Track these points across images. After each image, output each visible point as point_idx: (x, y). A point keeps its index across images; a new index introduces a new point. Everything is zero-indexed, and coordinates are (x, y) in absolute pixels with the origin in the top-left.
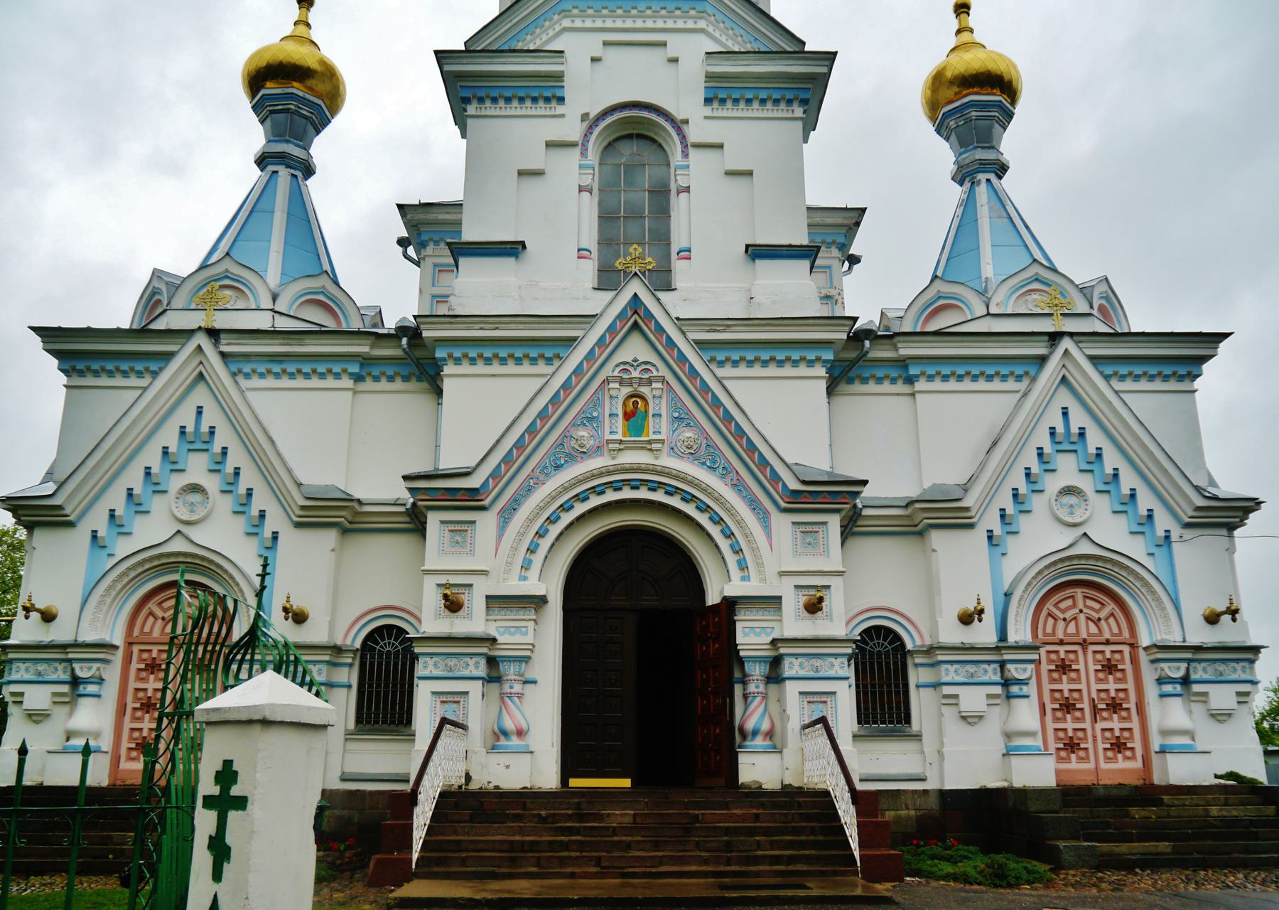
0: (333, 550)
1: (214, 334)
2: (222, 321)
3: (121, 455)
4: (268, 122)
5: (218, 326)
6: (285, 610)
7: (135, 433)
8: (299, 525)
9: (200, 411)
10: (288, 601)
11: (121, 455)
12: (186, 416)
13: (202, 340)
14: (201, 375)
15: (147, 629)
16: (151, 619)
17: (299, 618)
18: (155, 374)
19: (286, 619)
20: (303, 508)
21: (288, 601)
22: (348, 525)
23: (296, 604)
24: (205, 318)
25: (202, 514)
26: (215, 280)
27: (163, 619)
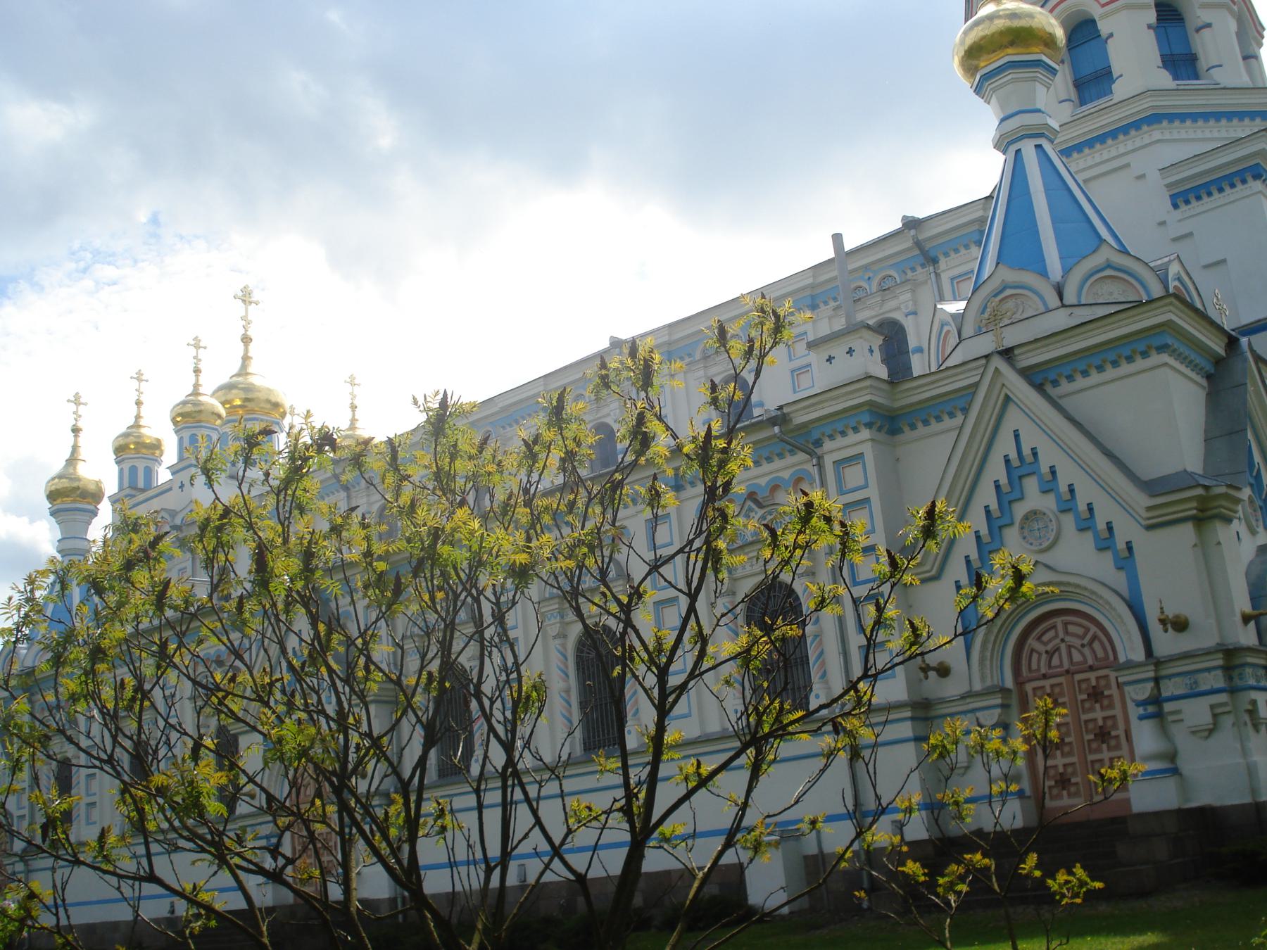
0: (1195, 545)
1: (1007, 353)
2: (1012, 337)
3: (964, 487)
4: (994, 100)
5: (1008, 343)
6: (1163, 622)
7: (971, 458)
8: (1149, 528)
9: (1017, 436)
10: (1162, 612)
11: (964, 487)
12: (1005, 445)
13: (998, 362)
14: (1007, 399)
15: (1034, 666)
16: (1035, 656)
17: (1180, 625)
18: (965, 411)
19: (1166, 631)
20: (1149, 509)
21: (1162, 612)
22: (1201, 515)
23: (1170, 613)
24: (994, 338)
25: (1052, 538)
26: (995, 296)
27: (1047, 652)
